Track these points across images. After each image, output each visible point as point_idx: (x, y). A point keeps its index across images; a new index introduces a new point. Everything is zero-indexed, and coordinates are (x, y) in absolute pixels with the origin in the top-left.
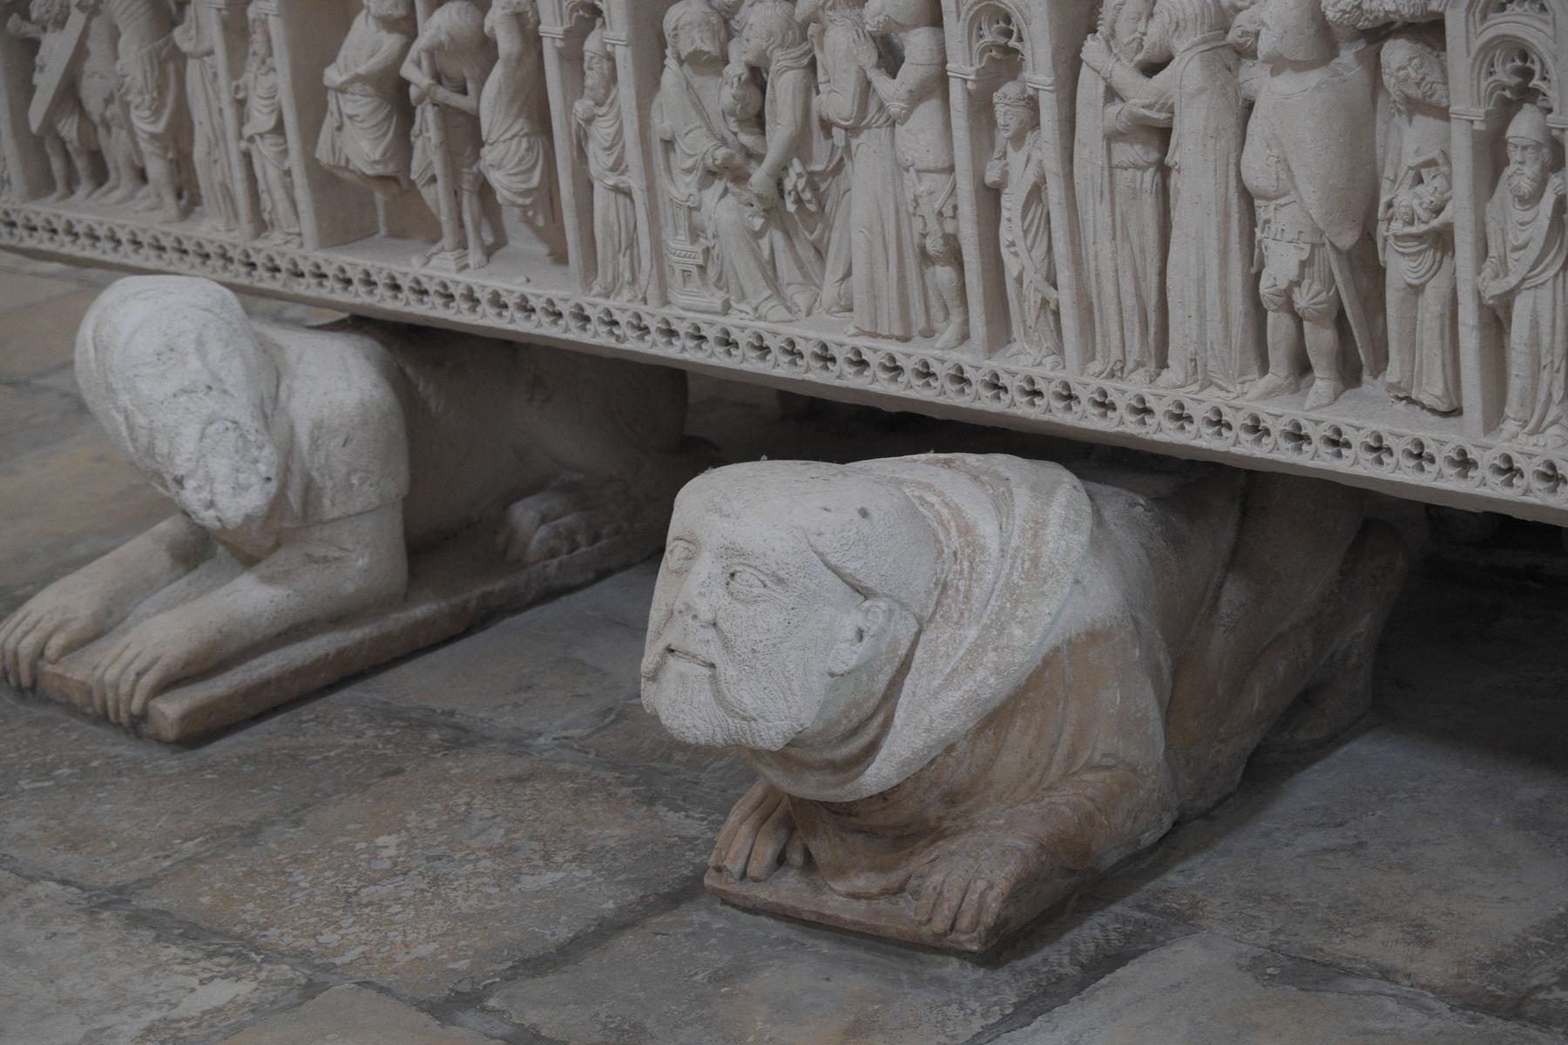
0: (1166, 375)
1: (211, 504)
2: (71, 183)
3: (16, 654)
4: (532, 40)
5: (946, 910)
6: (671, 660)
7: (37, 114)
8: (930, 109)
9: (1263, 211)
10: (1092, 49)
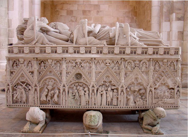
2: (15, 103)
3: (26, 131)
4: (59, 92)
5: (101, 132)
7: (14, 99)
9: (107, 97)
10: (99, 91)
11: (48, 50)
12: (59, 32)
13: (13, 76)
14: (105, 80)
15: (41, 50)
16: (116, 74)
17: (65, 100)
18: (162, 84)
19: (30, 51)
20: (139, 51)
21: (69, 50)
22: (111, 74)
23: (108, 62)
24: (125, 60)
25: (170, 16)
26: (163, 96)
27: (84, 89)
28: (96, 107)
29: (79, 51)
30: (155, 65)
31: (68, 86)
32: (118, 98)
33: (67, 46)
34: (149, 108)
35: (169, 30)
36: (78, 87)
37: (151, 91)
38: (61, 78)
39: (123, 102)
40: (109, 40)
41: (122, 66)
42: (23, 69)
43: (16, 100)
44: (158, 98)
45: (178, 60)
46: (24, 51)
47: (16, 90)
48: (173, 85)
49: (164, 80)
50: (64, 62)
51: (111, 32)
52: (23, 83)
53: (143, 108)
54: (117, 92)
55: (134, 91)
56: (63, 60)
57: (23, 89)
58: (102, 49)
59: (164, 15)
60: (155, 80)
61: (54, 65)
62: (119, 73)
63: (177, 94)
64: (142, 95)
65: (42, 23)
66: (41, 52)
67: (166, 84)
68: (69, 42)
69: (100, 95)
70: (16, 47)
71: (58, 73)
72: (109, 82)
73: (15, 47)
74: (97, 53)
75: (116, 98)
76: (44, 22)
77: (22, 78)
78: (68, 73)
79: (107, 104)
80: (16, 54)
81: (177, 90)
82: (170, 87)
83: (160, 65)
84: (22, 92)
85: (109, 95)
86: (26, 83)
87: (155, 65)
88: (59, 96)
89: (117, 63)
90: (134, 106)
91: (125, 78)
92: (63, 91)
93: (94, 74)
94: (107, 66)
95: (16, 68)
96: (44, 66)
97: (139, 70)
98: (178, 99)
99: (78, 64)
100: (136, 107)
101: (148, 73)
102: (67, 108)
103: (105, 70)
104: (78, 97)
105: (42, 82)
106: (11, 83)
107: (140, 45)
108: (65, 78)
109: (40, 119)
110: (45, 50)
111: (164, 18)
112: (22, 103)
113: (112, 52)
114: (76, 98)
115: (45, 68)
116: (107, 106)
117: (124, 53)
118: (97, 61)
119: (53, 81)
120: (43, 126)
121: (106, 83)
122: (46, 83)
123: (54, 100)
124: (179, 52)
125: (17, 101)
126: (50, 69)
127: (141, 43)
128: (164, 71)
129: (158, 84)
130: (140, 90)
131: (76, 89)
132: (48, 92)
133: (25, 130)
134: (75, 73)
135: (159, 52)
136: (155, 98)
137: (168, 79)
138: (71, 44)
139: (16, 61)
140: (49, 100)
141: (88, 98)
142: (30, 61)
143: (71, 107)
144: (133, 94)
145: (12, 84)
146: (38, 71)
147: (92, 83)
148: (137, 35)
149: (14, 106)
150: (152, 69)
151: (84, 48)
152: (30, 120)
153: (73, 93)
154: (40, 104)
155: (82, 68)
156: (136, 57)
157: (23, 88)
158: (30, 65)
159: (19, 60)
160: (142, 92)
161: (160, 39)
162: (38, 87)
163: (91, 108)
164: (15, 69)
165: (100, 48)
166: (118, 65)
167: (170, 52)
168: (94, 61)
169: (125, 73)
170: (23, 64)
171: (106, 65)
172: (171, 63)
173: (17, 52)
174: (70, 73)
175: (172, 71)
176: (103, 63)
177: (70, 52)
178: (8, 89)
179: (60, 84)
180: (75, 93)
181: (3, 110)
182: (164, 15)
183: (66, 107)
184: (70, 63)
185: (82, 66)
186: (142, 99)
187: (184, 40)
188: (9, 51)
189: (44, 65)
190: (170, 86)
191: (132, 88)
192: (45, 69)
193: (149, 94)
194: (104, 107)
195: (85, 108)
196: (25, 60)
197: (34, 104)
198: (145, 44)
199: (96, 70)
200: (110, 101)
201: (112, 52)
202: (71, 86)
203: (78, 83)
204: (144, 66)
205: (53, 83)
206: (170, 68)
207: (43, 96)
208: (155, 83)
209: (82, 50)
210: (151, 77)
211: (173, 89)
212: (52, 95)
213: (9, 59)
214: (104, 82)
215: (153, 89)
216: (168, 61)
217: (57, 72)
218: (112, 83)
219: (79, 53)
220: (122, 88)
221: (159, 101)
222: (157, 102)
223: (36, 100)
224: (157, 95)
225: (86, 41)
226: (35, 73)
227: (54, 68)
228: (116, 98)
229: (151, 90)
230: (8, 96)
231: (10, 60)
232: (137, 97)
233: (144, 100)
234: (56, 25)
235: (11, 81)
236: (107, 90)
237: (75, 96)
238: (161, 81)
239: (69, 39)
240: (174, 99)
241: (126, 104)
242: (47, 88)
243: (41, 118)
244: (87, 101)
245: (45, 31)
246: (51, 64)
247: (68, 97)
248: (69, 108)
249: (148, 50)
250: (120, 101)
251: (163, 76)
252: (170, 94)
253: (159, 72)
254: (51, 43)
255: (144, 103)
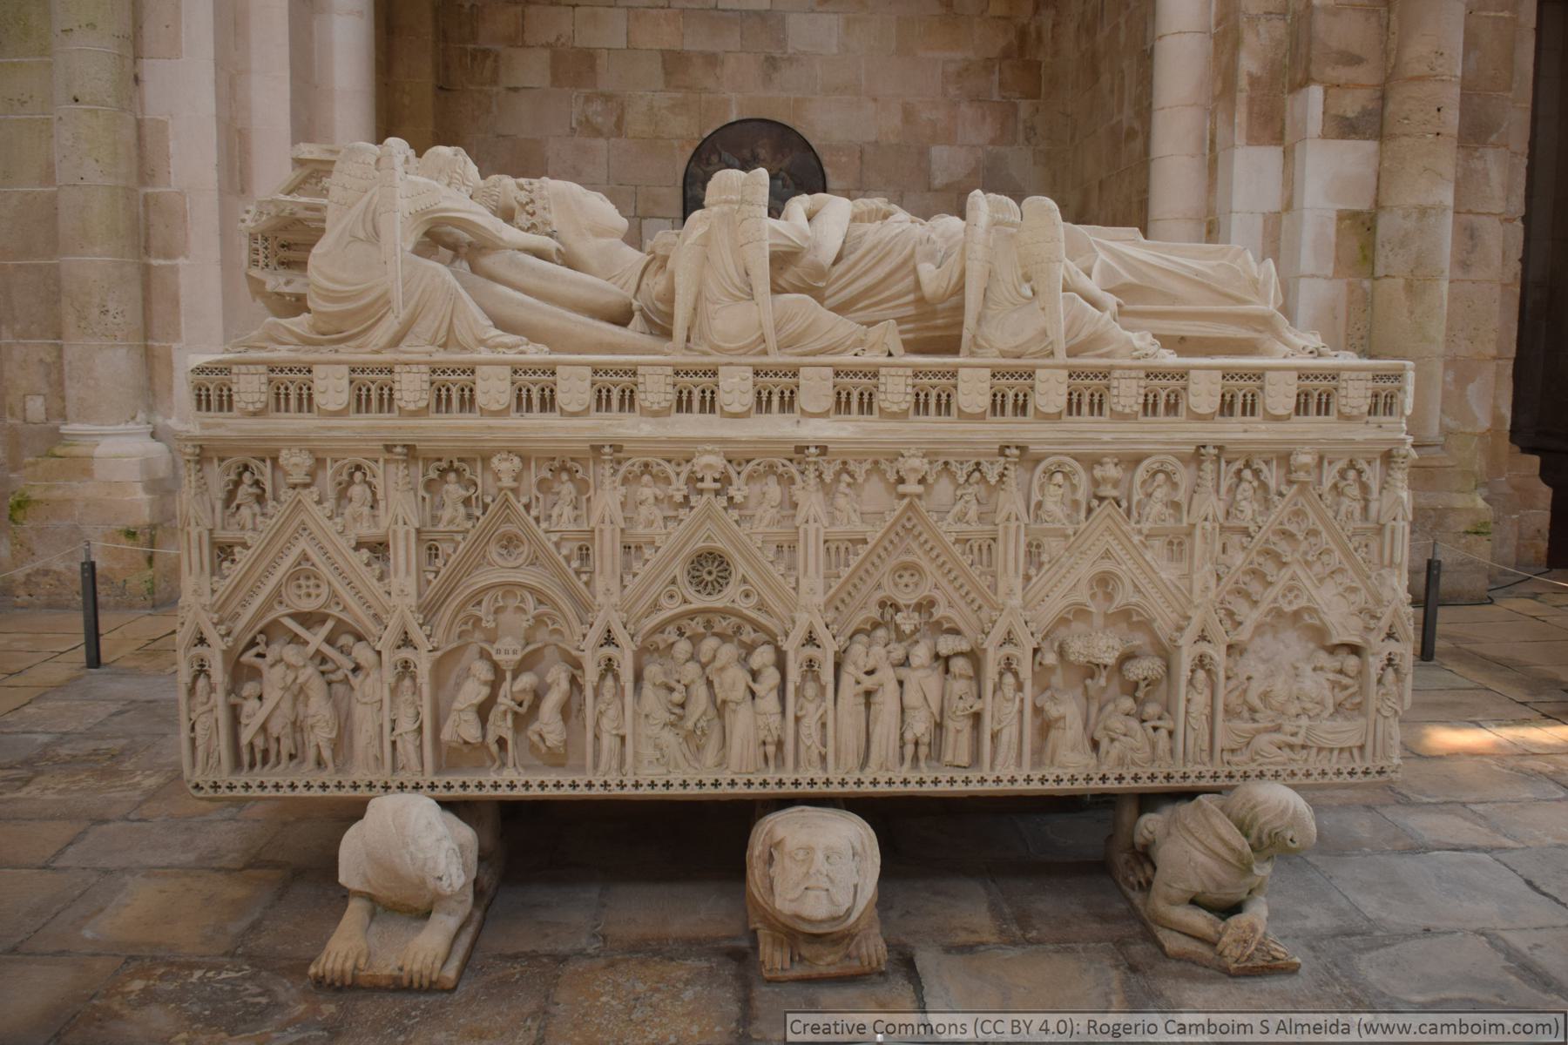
0: (868, 771)
1: (450, 885)
2: (252, 765)
3: (343, 971)
5: (874, 958)
6: (809, 892)
7: (245, 738)
8: (774, 695)
9: (908, 713)
11: (494, 389)
12: (558, 250)
13: (234, 571)
14: (888, 591)
15: (444, 392)
16: (963, 553)
17: (618, 740)
18: (1279, 613)
19: (359, 396)
20: (1127, 394)
21: (641, 387)
22: (934, 554)
23: (914, 470)
24: (1026, 456)
25: (1288, 103)
26: (1281, 699)
27: (745, 660)
28: (828, 782)
29: (712, 398)
30: (1232, 490)
31: (639, 639)
32: (977, 718)
33: (631, 364)
34: (1188, 784)
35: (1273, 202)
36: (710, 644)
37: (1201, 662)
38: (587, 584)
39: (1015, 740)
40: (911, 311)
41: (1011, 501)
42: (311, 525)
43: (260, 743)
44: (1253, 710)
45: (1394, 452)
46: (310, 395)
47: (256, 674)
48: (1357, 623)
49: (1291, 590)
50: (608, 471)
51: (930, 257)
52: (309, 620)
53: (1149, 784)
54: (970, 678)
55: (1091, 670)
56: (604, 461)
57: (310, 670)
58: (874, 381)
59: (1242, 98)
60: (1229, 593)
61: (534, 491)
62: (985, 548)
63: (1380, 681)
64: (1140, 694)
65: (441, 186)
66: (442, 401)
67: (1306, 617)
68: (630, 326)
69: (856, 695)
70: (252, 369)
71: (565, 551)
72: (919, 607)
73: (243, 369)
74: (838, 410)
75: (968, 716)
76: (449, 185)
77: (299, 586)
78: (638, 548)
79: (902, 758)
80: (255, 414)
81: (1384, 655)
82: (1336, 640)
83: (1264, 486)
84: (301, 690)
85: (922, 700)
86: (330, 624)
87: (1232, 490)
88: (575, 707)
89: (977, 474)
90: (1086, 766)
91: (1028, 578)
92: (602, 677)
93: (811, 555)
94: (906, 501)
95: (254, 515)
96: (467, 502)
97: (1125, 527)
98: (1386, 717)
99: (709, 490)
100: (1104, 778)
101: (1186, 546)
102: (629, 791)
103: (893, 525)
104: (704, 713)
105: (449, 612)
106: (223, 629)
107: (1135, 354)
108: (615, 586)
109: (445, 883)
110: (471, 390)
111: (1241, 117)
112: (303, 761)
113: (943, 401)
114: (690, 724)
115: (469, 516)
116: (906, 771)
117: (1021, 408)
118: (837, 466)
119: (530, 603)
120: (462, 927)
121: (899, 618)
122: (479, 619)
123: (535, 738)
124: (1400, 395)
125: (266, 752)
126: (508, 520)
127: (1134, 337)
128: (1292, 528)
129: (1251, 617)
130: (1128, 657)
131: (693, 657)
132: (495, 686)
133: (338, 967)
134: (687, 550)
135: (1268, 401)
136: (1229, 712)
137: (1321, 580)
138: (647, 341)
139: (253, 463)
140: (501, 742)
141: (778, 717)
142: (358, 468)
143: (660, 783)
144: (1080, 690)
145: (228, 634)
146: (419, 540)
147: (803, 619)
148: (1107, 271)
149: (247, 787)
150: (1210, 517)
151: (750, 375)
152: (368, 890)
153: (671, 690)
154: (438, 770)
155: (735, 514)
156: (1106, 437)
157: (312, 658)
158: (357, 491)
159: (275, 460)
160: (1137, 670)
161: (1267, 303)
162: (423, 652)
163: (800, 789)
164: (249, 525)
165: (856, 375)
166: (982, 490)
167: (1344, 401)
168: (815, 463)
169: (1029, 545)
170: (306, 486)
171: (901, 488)
172: (1343, 474)
173: (259, 405)
174: (648, 552)
175: (1350, 527)
176: (875, 478)
177: (647, 404)
178: (202, 670)
179: (585, 629)
180: (686, 687)
181: (146, 801)
182: (1244, 95)
183: (622, 785)
184: (646, 478)
185: (731, 499)
186: (1143, 721)
187: (1379, 271)
188: (203, 392)
189: (464, 493)
190: (1334, 632)
191: (1078, 650)
192: (469, 525)
193: (1191, 682)
194: (882, 780)
195: (756, 790)
196: (320, 462)
197: (394, 769)
198: (1166, 341)
199: (832, 524)
200: (926, 739)
201: (943, 401)
202: (658, 638)
203: (709, 616)
204: (1159, 494)
205: (532, 622)
206: (1338, 504)
207: (461, 711)
208: (1230, 614)
209: (736, 387)
210: (1203, 574)
211: (1355, 650)
212: (520, 705)
213: (198, 451)
214: (882, 604)
215: (1217, 654)
216: (1321, 459)
217: (557, 545)
218: (940, 612)
219: (712, 410)
220: (1008, 649)
221: (1258, 732)
222: (1248, 743)
223: (408, 747)
224: (1245, 691)
225: (761, 326)
226: (396, 554)
227: (534, 512)
228: (968, 716)
229: (1207, 661)
230: (203, 718)
231: (210, 460)
232: (1110, 707)
233: (1155, 729)
234: (539, 203)
235: (224, 613)
236: (905, 662)
237: (682, 706)
238: (1275, 600)
239: (636, 304)
240: (1361, 721)
241: (1033, 752)
242: (484, 655)
243: (450, 876)
244: (769, 739)
245: (464, 250)
246: (513, 490)
247: (636, 714)
248: (645, 791)
249: (1192, 387)
250: (993, 737)
251: (1285, 564)
252: (1334, 685)
253: (1257, 537)
254: (509, 339)
255: (1154, 746)
